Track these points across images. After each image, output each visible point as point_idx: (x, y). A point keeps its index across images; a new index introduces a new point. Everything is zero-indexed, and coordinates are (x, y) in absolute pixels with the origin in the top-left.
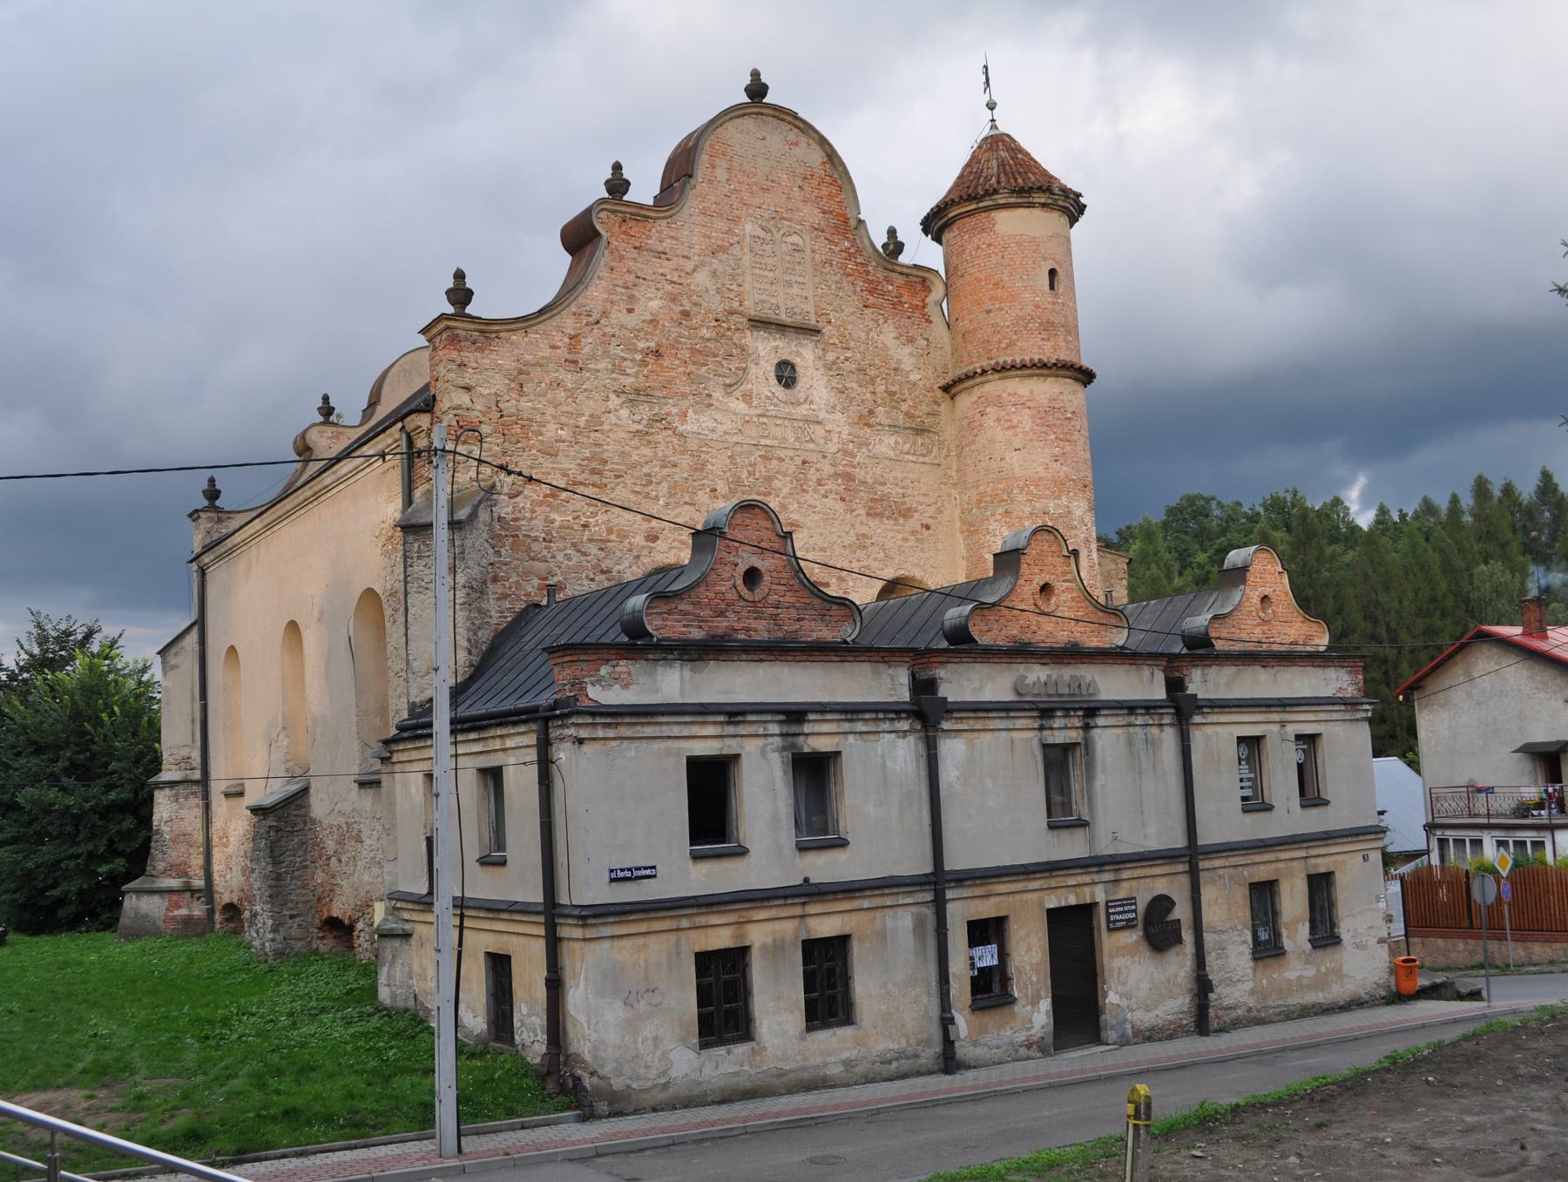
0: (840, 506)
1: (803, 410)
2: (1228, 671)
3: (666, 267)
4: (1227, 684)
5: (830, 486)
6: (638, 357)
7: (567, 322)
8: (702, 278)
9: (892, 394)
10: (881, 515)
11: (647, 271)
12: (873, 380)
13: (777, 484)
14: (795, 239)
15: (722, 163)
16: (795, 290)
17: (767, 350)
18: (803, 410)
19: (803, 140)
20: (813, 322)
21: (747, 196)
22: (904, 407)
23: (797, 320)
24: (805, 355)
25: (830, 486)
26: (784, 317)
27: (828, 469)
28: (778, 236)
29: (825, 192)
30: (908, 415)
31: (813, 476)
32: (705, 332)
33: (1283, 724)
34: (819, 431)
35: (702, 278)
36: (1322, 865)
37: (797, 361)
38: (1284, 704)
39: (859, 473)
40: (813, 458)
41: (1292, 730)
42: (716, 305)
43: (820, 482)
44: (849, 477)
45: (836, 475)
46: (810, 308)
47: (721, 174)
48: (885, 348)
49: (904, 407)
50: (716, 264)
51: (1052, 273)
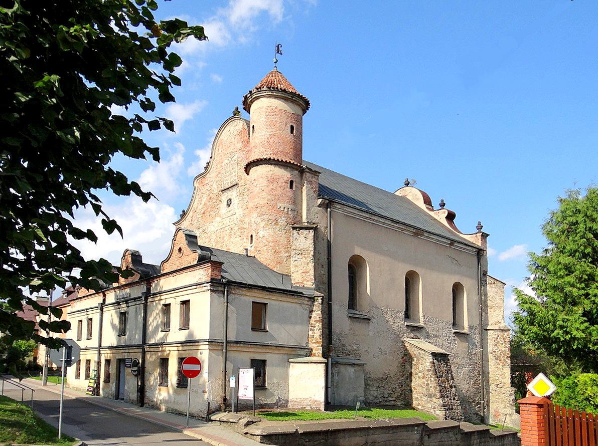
3: (208, 187)
5: (238, 233)
6: (201, 216)
7: (191, 214)
8: (215, 186)
11: (204, 191)
13: (225, 238)
14: (235, 157)
15: (221, 147)
17: (225, 197)
24: (233, 194)
26: (230, 185)
27: (236, 228)
28: (230, 160)
32: (214, 201)
35: (215, 186)
42: (216, 191)
46: (236, 178)
47: (220, 151)
50: (218, 179)
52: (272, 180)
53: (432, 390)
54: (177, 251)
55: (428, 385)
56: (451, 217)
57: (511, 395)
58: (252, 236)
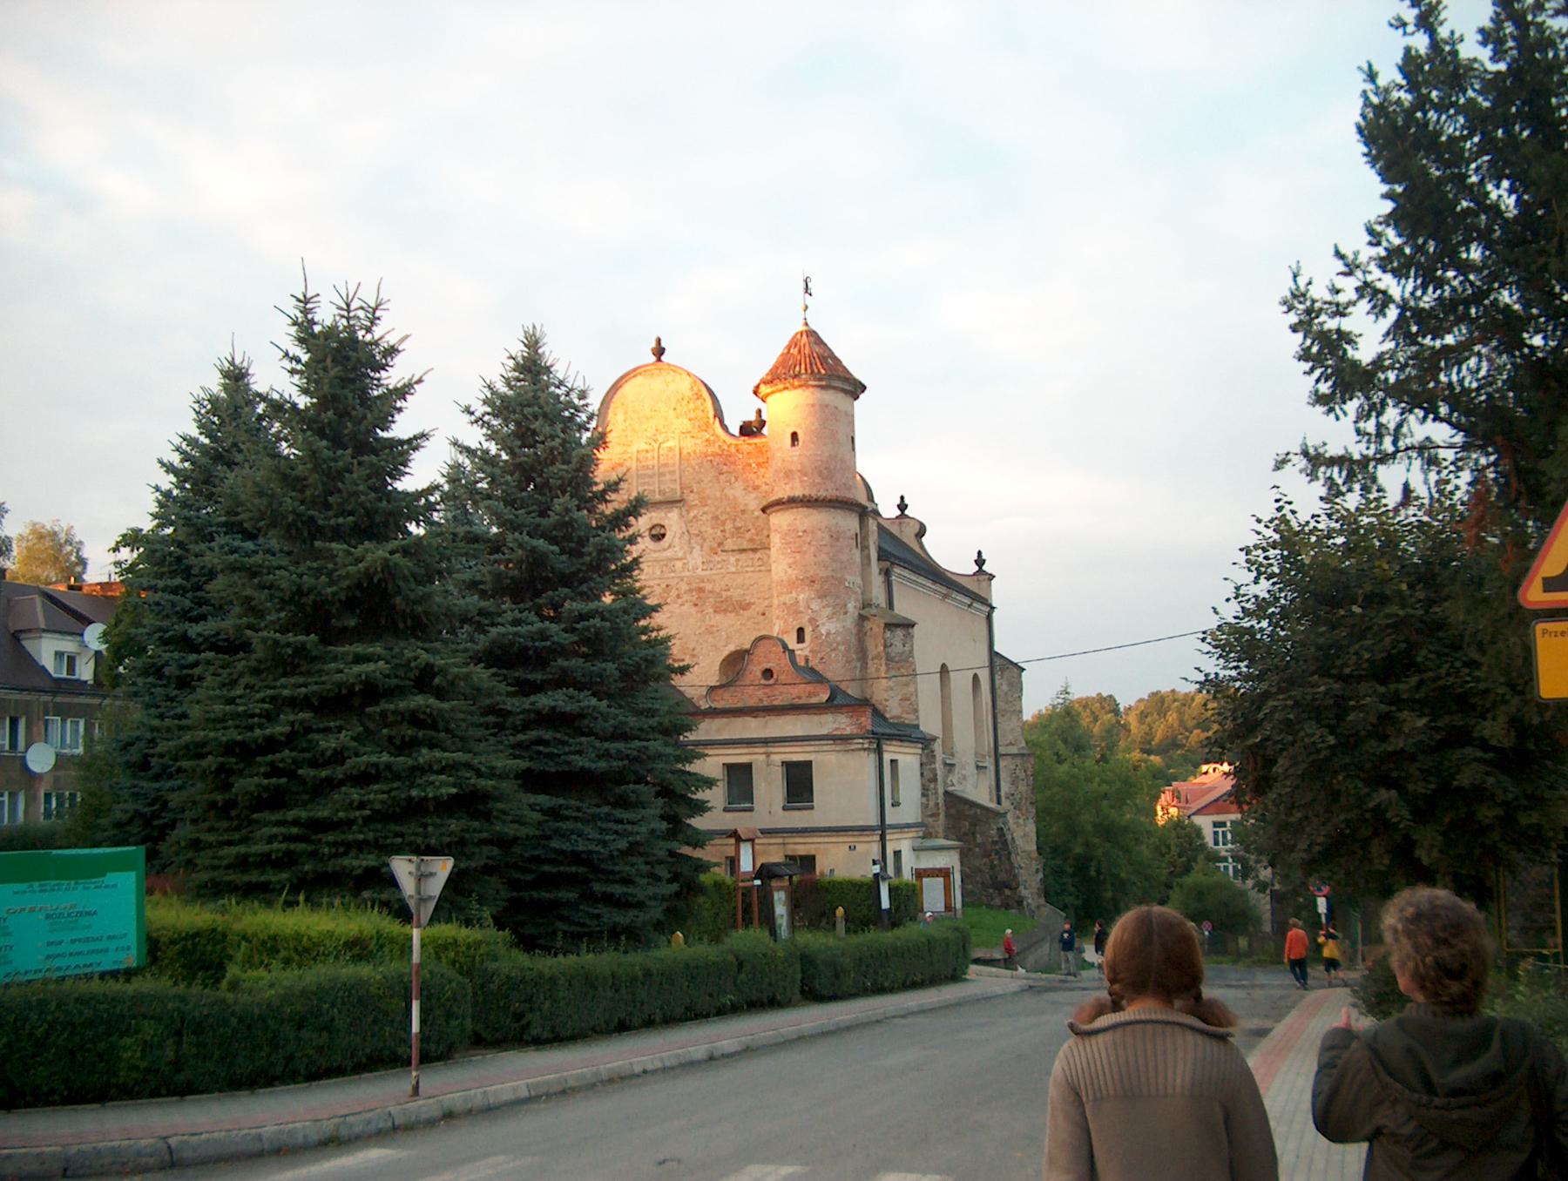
0: (693, 610)
1: (669, 553)
2: (719, 722)
4: (718, 731)
9: (738, 528)
10: (725, 611)
12: (723, 523)
16: (668, 477)
18: (669, 553)
19: (678, 378)
20: (678, 496)
21: (636, 426)
22: (748, 535)
23: (669, 496)
25: (685, 597)
27: (684, 587)
29: (692, 406)
30: (752, 540)
31: (674, 593)
33: (768, 755)
34: (679, 564)
36: (802, 850)
37: (666, 523)
38: (766, 742)
39: (708, 587)
40: (673, 583)
41: (777, 759)
43: (678, 596)
44: (701, 590)
45: (690, 590)
47: (620, 418)
48: (735, 498)
49: (748, 535)
51: (794, 436)
52: (835, 537)
53: (1002, 876)
54: (759, 674)
55: (992, 867)
56: (922, 531)
57: (1037, 871)
58: (801, 631)
